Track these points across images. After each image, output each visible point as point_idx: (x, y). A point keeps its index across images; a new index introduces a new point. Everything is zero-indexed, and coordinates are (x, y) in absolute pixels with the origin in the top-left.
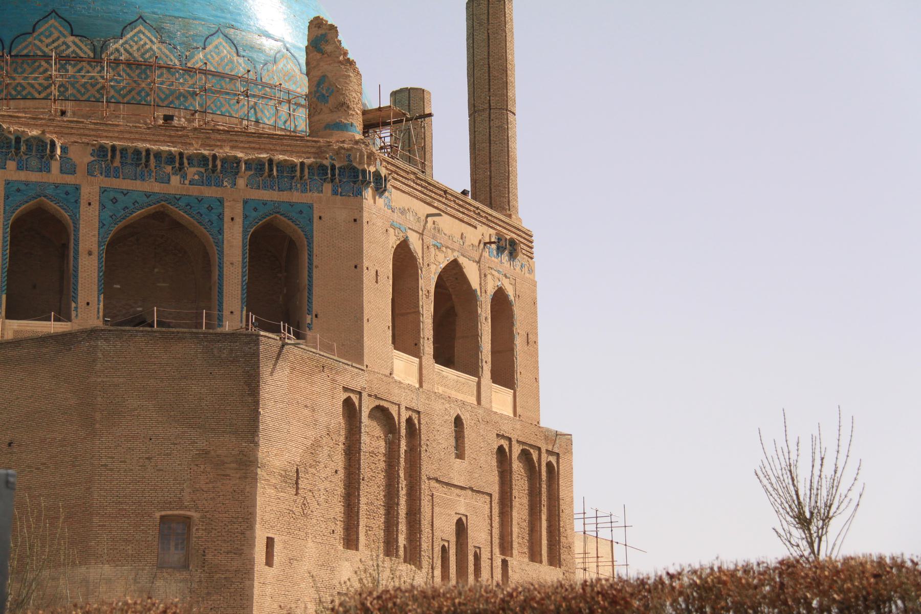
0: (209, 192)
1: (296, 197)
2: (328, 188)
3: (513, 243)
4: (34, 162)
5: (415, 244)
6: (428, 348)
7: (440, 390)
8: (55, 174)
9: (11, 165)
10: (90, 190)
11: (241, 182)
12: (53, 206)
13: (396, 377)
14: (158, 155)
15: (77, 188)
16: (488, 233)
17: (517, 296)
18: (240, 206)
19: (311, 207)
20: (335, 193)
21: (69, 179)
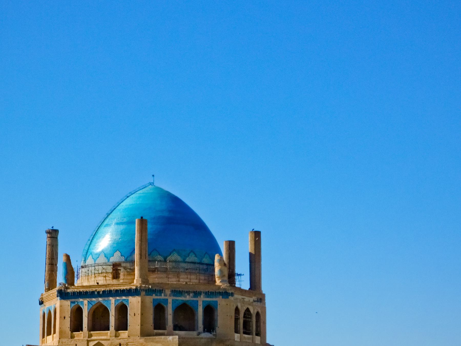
0: (195, 299)
1: (214, 299)
2: (221, 297)
3: (261, 299)
4: (159, 294)
5: (239, 307)
6: (242, 331)
7: (244, 340)
8: (163, 297)
9: (154, 295)
10: (170, 300)
11: (202, 296)
12: (162, 304)
13: (236, 340)
14: (184, 291)
15: (167, 299)
16: (255, 298)
17: (262, 312)
18: (201, 303)
19: (217, 302)
20: (222, 298)
21: (166, 298)
